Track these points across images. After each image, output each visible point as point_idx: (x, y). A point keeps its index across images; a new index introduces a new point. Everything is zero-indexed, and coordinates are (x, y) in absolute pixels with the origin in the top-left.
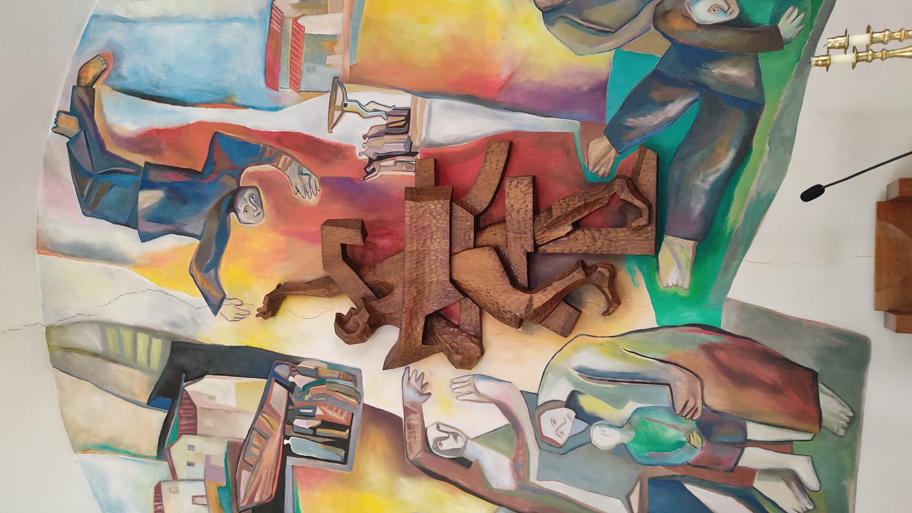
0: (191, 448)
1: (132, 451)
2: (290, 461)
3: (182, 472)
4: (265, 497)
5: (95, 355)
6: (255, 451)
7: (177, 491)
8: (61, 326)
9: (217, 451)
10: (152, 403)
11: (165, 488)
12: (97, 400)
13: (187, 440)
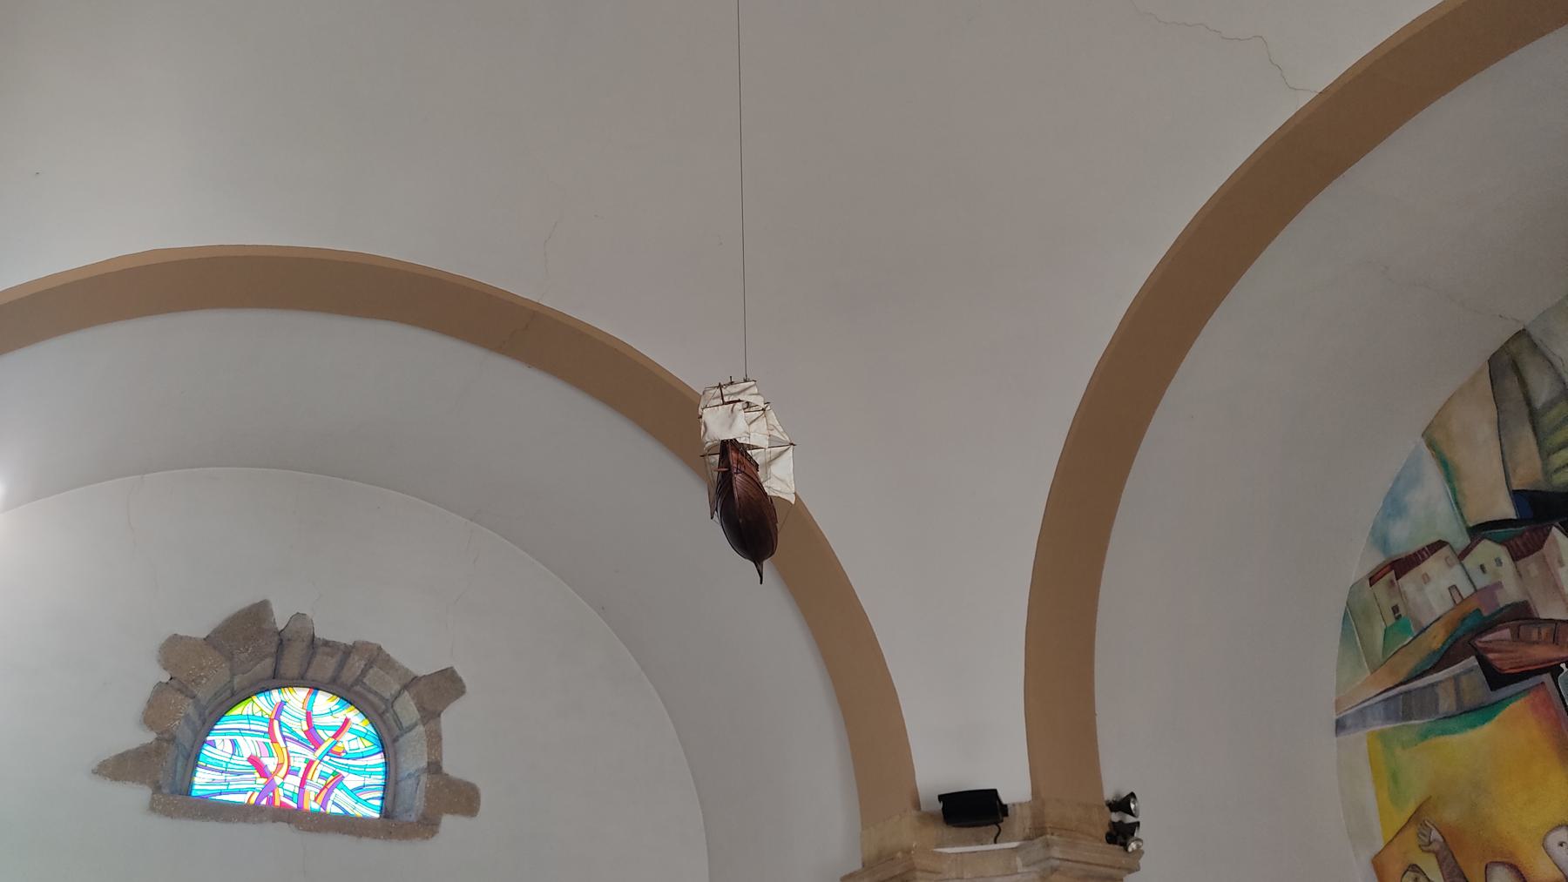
0: (1499, 562)
1: (1459, 497)
2: (1546, 678)
3: (1470, 562)
4: (1497, 664)
5: (1528, 402)
6: (1535, 636)
7: (1450, 566)
8: (1535, 346)
9: (1511, 592)
10: (1518, 496)
11: (1445, 551)
12: (1485, 432)
13: (1502, 552)
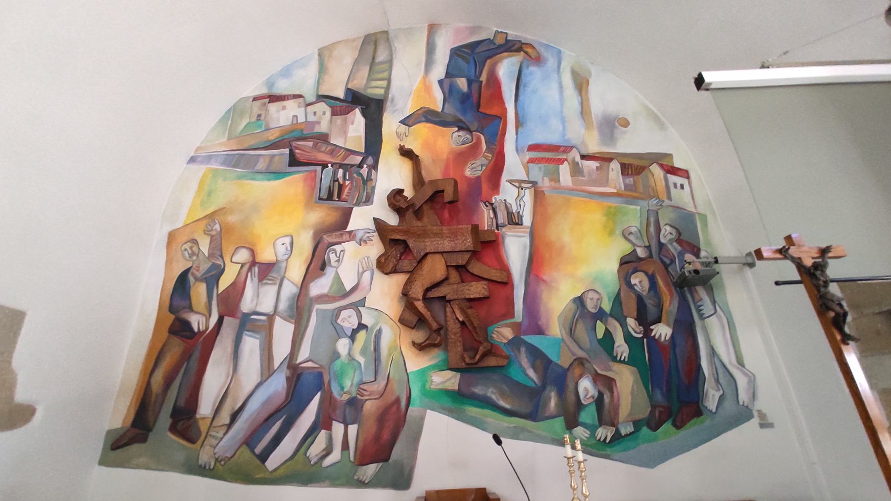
0: (324, 113)
2: (319, 168)
3: (310, 109)
4: (298, 156)
5: (374, 58)
6: (323, 149)
7: (299, 107)
8: (388, 39)
9: (323, 127)
10: (348, 91)
11: (301, 100)
